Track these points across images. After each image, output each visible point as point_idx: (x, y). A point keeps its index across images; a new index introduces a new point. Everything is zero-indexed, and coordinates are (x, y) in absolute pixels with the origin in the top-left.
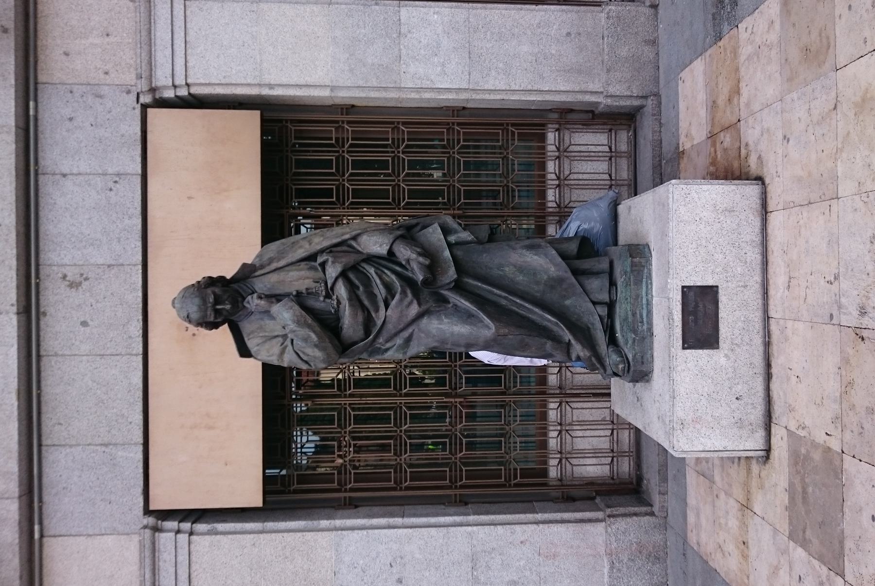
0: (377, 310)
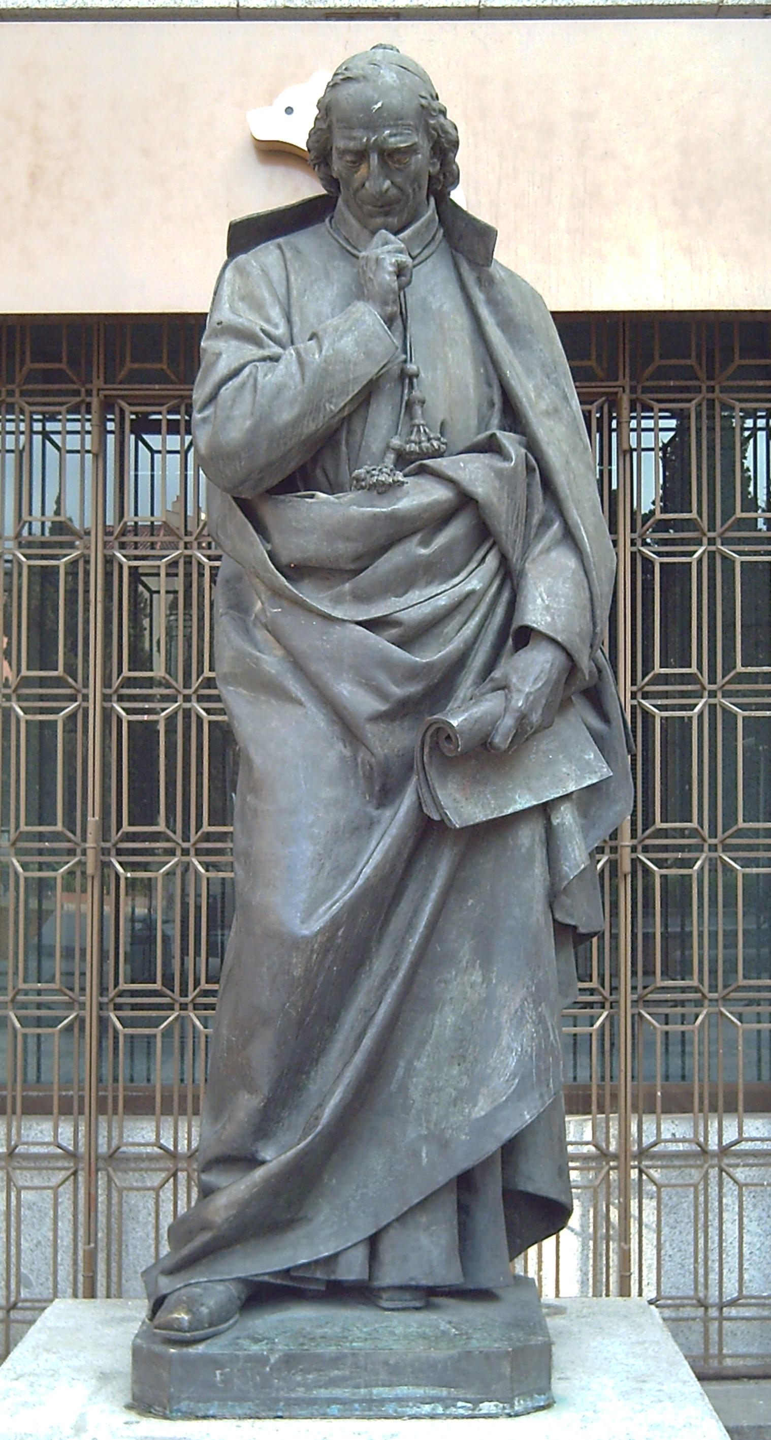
0: (362, 597)
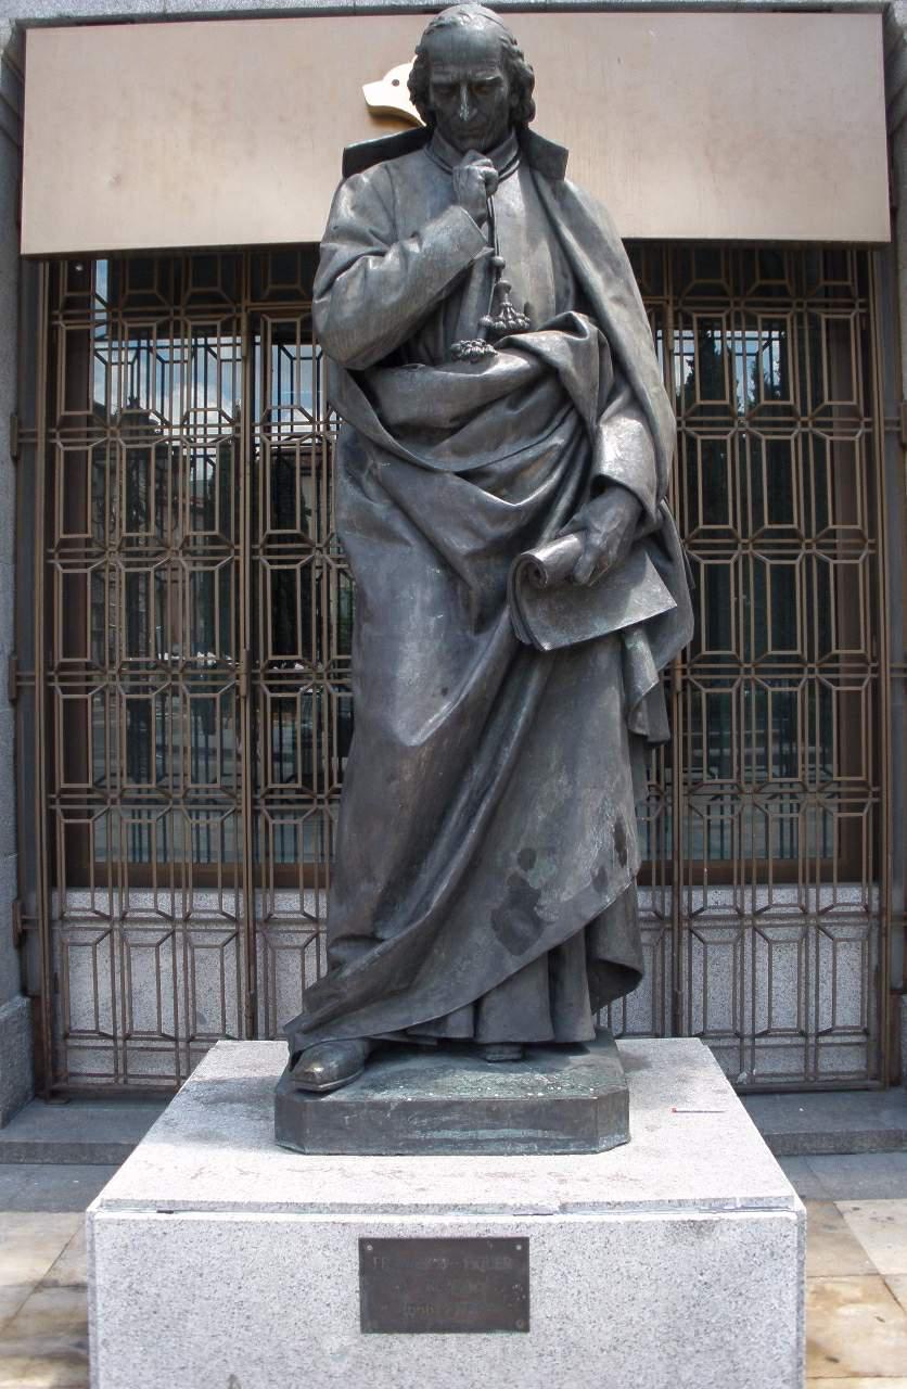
0: (461, 452)
